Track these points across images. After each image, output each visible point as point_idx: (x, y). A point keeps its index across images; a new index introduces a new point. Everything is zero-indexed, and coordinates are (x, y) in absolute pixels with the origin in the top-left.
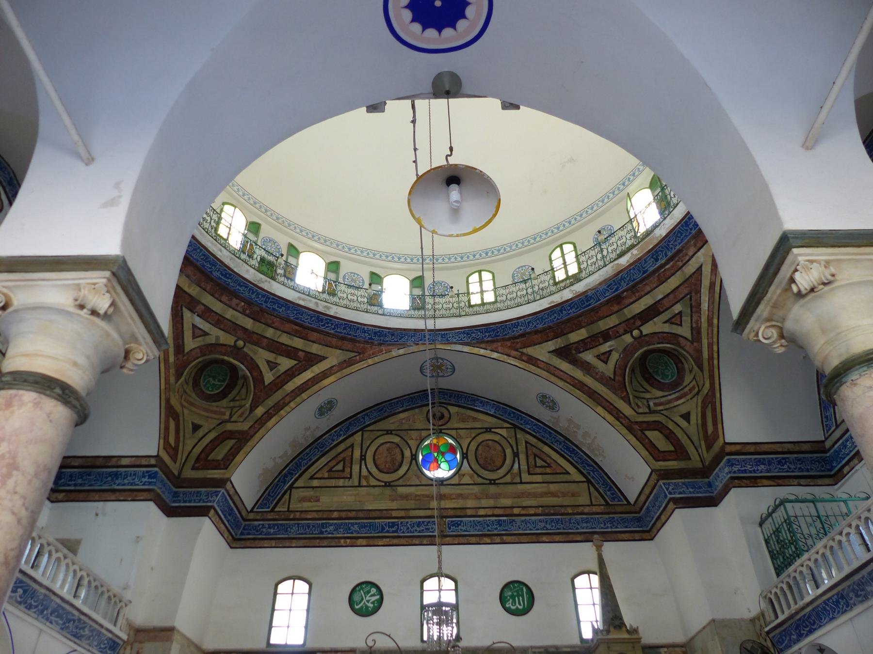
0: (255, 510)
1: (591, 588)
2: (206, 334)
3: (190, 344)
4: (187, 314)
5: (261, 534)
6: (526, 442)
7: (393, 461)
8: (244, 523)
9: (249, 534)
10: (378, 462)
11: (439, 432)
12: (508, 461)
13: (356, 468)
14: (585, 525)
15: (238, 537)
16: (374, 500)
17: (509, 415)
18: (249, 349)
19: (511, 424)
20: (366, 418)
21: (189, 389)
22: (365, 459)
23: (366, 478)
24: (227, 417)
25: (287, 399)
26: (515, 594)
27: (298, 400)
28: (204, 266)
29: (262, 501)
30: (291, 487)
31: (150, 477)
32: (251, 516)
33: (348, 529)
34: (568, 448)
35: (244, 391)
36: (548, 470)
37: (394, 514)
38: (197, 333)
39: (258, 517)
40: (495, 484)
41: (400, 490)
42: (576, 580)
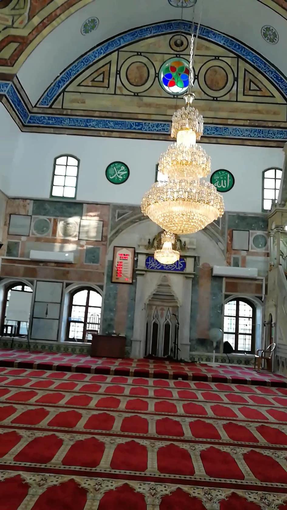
0: (37, 106)
1: (275, 179)
5: (43, 123)
6: (245, 70)
7: (141, 77)
8: (30, 115)
9: (34, 123)
10: (129, 77)
11: (177, 56)
12: (229, 84)
13: (112, 80)
14: (279, 135)
15: (26, 124)
16: (125, 105)
17: (235, 47)
19: (235, 54)
20: (122, 40)
22: (120, 74)
23: (120, 88)
24: (10, 23)
25: (58, 12)
26: (222, 178)
27: (67, 13)
29: (43, 99)
30: (64, 91)
32: (35, 110)
33: (105, 125)
34: (277, 77)
36: (259, 93)
37: (140, 116)
39: (40, 112)
40: (217, 100)
41: (146, 100)
42: (265, 173)
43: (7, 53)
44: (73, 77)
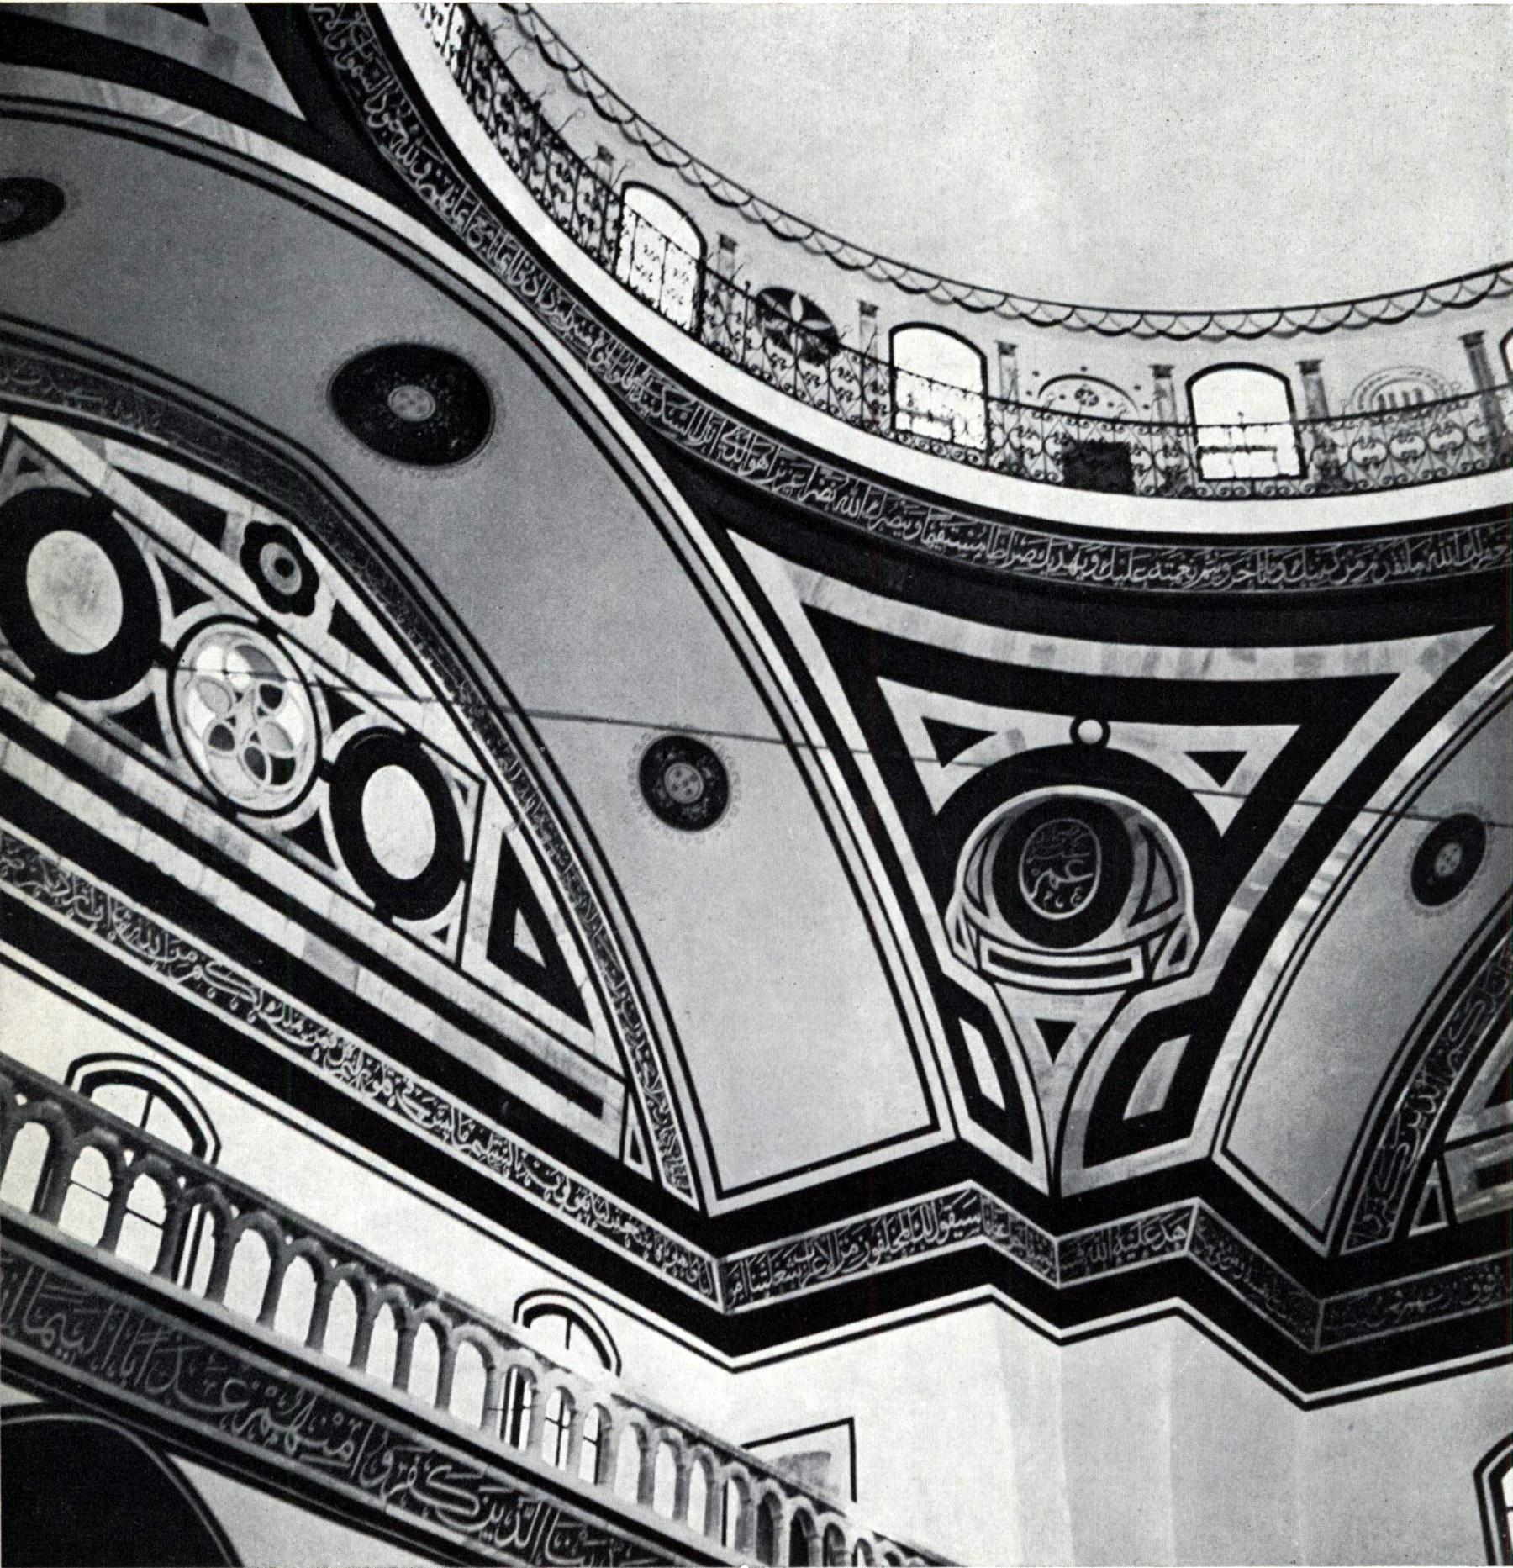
2: (973, 737)
3: (941, 783)
4: (893, 691)
18: (1127, 737)
21: (996, 923)
24: (1137, 973)
28: (888, 531)
30: (1438, 1147)
31: (961, 1213)
35: (1160, 875)
38: (950, 740)
43: (1150, 1090)
44: (1457, 1076)
